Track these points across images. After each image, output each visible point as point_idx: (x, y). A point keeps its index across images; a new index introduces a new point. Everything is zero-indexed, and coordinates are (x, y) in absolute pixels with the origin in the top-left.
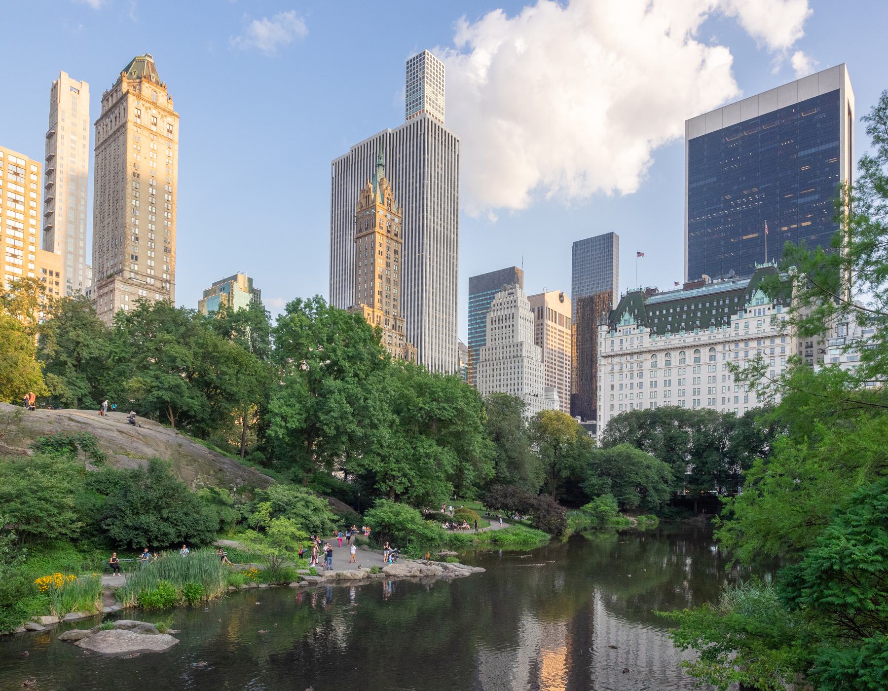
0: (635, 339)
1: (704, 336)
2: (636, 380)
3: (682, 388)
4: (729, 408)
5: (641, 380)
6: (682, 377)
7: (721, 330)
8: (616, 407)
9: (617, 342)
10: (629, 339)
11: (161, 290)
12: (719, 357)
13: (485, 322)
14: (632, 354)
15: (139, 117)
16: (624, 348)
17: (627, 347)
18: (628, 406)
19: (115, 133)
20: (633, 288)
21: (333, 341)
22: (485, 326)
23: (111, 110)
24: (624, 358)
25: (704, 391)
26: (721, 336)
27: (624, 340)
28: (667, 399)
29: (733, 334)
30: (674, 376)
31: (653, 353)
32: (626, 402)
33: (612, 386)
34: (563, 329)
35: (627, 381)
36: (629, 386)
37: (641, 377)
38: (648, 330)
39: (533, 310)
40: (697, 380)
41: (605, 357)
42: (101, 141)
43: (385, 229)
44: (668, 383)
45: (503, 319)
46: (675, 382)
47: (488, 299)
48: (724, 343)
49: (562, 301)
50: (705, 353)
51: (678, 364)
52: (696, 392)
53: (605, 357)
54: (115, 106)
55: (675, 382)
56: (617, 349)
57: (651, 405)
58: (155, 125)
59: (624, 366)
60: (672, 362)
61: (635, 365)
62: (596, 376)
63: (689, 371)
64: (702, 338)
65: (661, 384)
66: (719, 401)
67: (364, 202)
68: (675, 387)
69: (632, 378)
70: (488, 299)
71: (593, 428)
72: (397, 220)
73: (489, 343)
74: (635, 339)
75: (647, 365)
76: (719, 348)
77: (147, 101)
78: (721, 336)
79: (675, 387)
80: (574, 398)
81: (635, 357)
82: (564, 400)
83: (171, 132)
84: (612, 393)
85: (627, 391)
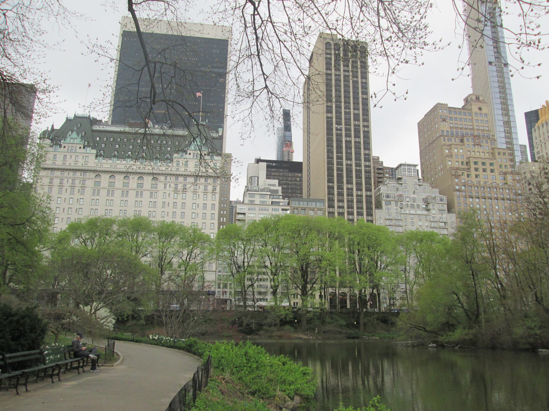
1: (148, 166)
2: (77, 196)
10: (73, 157)
12: (161, 186)
14: (75, 170)
16: (67, 164)
17: (70, 162)
27: (68, 157)
37: (83, 194)
38: (94, 151)
50: (148, 181)
59: (65, 181)
75: (90, 183)
81: (78, 174)
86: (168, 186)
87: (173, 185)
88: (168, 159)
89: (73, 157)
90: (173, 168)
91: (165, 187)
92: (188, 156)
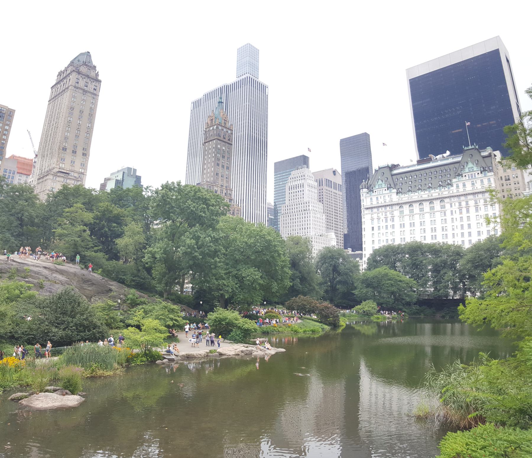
0: (387, 196)
1: (435, 193)
2: (390, 223)
3: (423, 227)
4: (458, 241)
5: (393, 223)
6: (422, 220)
7: (446, 189)
8: (376, 242)
9: (374, 199)
10: (382, 197)
11: (76, 179)
12: (448, 206)
13: (285, 189)
14: (385, 206)
15: (78, 83)
16: (380, 202)
17: (381, 201)
18: (385, 241)
19: (62, 92)
20: (383, 164)
21: (186, 207)
22: (285, 192)
23: (62, 80)
24: (380, 209)
25: (439, 229)
26: (447, 193)
27: (379, 198)
28: (412, 236)
29: (455, 191)
30: (417, 219)
31: (400, 205)
32: (384, 238)
33: (373, 228)
34: (337, 192)
35: (383, 224)
36: (384, 227)
37: (393, 221)
38: (395, 191)
39: (317, 181)
40: (433, 222)
41: (367, 208)
42: (53, 96)
43: (222, 136)
44: (412, 225)
45: (296, 187)
46: (417, 224)
47: (286, 175)
48: (450, 197)
49: (335, 174)
50: (437, 205)
51: (408, 213)
52: (434, 230)
53: (367, 208)
54: (64, 78)
55: (417, 224)
56: (375, 203)
57: (401, 241)
58: (87, 87)
60: (414, 210)
61: (388, 213)
62: (361, 222)
63: (427, 216)
64: (434, 195)
65: (407, 225)
66: (450, 236)
67: (209, 122)
68: (418, 227)
69: (386, 221)
70: (286, 175)
71: (361, 256)
72: (229, 132)
73: (287, 202)
74: (387, 196)
75: (396, 213)
76: (447, 200)
77: (83, 75)
78: (447, 193)
79: (418, 227)
80: (345, 236)
81: (388, 208)
82: (339, 241)
83: (96, 90)
84: (373, 232)
85: (383, 230)
86: (453, 205)
87: (457, 204)
88: (448, 184)
89: (382, 197)
90: (453, 190)
91: (451, 206)
92: (464, 178)
